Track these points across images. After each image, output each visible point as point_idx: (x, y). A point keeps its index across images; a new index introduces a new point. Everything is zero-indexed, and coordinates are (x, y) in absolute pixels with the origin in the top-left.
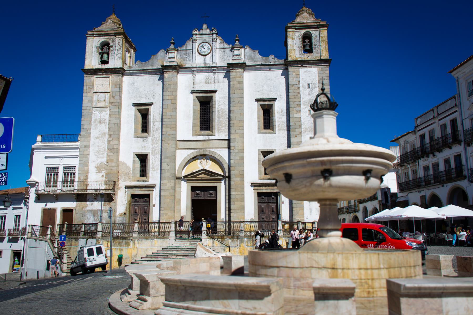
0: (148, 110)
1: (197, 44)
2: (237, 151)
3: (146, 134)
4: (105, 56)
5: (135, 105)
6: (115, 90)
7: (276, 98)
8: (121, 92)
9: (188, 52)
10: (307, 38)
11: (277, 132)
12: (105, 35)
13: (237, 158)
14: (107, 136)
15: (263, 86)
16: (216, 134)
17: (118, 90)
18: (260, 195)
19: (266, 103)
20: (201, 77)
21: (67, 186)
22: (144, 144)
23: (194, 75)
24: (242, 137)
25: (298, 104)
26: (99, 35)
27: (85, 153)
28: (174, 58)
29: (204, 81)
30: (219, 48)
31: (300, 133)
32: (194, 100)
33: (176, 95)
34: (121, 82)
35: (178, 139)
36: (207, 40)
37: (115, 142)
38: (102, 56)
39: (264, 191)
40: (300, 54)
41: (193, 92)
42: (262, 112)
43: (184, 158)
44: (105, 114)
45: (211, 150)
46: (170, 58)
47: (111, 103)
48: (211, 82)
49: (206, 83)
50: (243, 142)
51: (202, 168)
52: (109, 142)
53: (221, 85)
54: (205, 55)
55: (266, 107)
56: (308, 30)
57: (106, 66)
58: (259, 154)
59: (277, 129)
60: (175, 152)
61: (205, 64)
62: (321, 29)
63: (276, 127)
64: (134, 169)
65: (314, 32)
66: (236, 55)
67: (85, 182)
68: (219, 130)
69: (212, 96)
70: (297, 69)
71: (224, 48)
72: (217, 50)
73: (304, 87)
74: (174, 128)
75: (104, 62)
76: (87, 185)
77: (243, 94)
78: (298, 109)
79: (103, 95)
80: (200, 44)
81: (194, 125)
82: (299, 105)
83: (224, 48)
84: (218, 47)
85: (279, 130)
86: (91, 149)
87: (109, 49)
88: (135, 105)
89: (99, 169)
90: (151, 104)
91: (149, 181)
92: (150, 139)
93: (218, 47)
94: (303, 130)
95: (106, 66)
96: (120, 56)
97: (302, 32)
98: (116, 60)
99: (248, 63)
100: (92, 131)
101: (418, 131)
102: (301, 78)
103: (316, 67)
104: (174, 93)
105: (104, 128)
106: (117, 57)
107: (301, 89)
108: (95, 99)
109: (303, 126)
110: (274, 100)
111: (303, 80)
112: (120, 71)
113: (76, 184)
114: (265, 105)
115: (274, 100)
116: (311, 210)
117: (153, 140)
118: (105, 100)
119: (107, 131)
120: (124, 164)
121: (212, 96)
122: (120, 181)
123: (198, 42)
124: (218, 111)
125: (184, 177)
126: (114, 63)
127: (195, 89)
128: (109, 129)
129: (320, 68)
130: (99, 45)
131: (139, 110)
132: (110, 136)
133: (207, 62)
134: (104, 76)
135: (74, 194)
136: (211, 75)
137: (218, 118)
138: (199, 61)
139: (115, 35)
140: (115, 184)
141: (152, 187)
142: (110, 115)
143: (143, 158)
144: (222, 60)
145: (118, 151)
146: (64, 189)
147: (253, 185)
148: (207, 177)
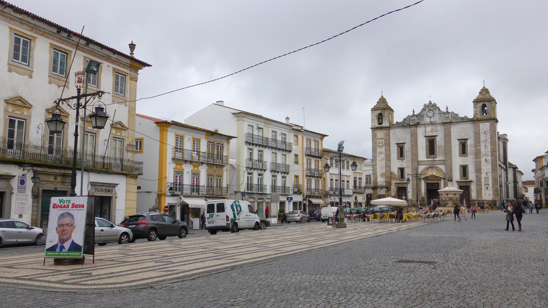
0: (403, 146)
1: (426, 112)
2: (448, 166)
3: (402, 158)
4: (380, 120)
5: (397, 144)
6: (386, 137)
7: (468, 139)
8: (389, 138)
9: (422, 116)
10: (484, 106)
11: (469, 155)
12: (380, 110)
13: (448, 169)
14: (384, 160)
15: (461, 132)
16: (438, 157)
17: (388, 137)
19: (463, 141)
20: (429, 129)
22: (402, 163)
23: (425, 128)
24: (451, 159)
25: (479, 142)
26: (377, 110)
27: (375, 168)
28: (415, 120)
29: (430, 131)
30: (438, 113)
31: (480, 156)
32: (426, 140)
33: (417, 139)
34: (389, 132)
35: (419, 160)
36: (431, 109)
37: (389, 163)
38: (379, 121)
39: (463, 185)
40: (480, 116)
41: (425, 137)
43: (421, 170)
44: (383, 149)
46: (413, 120)
47: (385, 144)
48: (434, 132)
49: (432, 132)
50: (451, 162)
51: (431, 174)
52: (386, 163)
53: (439, 132)
54: (430, 118)
56: (484, 103)
57: (381, 125)
58: (460, 167)
59: (469, 154)
60: (418, 167)
61: (431, 122)
62: (491, 102)
63: (468, 152)
64: (398, 175)
65: (487, 104)
66: (447, 117)
67: (375, 182)
68: (439, 155)
69: (435, 138)
71: (440, 113)
72: (437, 114)
73: (482, 133)
74: (417, 156)
77: (451, 137)
78: (479, 144)
79: (381, 140)
81: (427, 153)
82: (480, 142)
83: (440, 113)
84: (437, 113)
85: (470, 154)
86: (378, 166)
87: (382, 116)
88: (397, 144)
89: (382, 175)
90: (404, 143)
92: (405, 160)
93: (437, 113)
94: (482, 155)
95: (381, 125)
96: (388, 120)
97: (481, 104)
98: (386, 123)
99: (453, 121)
100: (377, 158)
102: (481, 128)
103: (488, 122)
104: (416, 138)
105: (383, 156)
106: (386, 121)
107: (481, 134)
108: (377, 142)
109: (482, 153)
110: (467, 139)
111: (481, 129)
112: (389, 128)
113: (372, 183)
115: (467, 139)
116: (485, 194)
117: (406, 161)
118: (382, 143)
119: (384, 157)
120: (394, 173)
121: (435, 138)
122: (392, 181)
123: (427, 111)
124: (438, 146)
125: (423, 178)
126: (385, 124)
127: (426, 135)
128: (385, 157)
130: (377, 114)
131: (399, 146)
132: (386, 160)
133: (432, 121)
136: (434, 127)
137: (438, 149)
138: (428, 120)
139: (385, 109)
140: (390, 183)
142: (385, 150)
143: (402, 170)
144: (439, 119)
145: (390, 167)
147: (457, 182)
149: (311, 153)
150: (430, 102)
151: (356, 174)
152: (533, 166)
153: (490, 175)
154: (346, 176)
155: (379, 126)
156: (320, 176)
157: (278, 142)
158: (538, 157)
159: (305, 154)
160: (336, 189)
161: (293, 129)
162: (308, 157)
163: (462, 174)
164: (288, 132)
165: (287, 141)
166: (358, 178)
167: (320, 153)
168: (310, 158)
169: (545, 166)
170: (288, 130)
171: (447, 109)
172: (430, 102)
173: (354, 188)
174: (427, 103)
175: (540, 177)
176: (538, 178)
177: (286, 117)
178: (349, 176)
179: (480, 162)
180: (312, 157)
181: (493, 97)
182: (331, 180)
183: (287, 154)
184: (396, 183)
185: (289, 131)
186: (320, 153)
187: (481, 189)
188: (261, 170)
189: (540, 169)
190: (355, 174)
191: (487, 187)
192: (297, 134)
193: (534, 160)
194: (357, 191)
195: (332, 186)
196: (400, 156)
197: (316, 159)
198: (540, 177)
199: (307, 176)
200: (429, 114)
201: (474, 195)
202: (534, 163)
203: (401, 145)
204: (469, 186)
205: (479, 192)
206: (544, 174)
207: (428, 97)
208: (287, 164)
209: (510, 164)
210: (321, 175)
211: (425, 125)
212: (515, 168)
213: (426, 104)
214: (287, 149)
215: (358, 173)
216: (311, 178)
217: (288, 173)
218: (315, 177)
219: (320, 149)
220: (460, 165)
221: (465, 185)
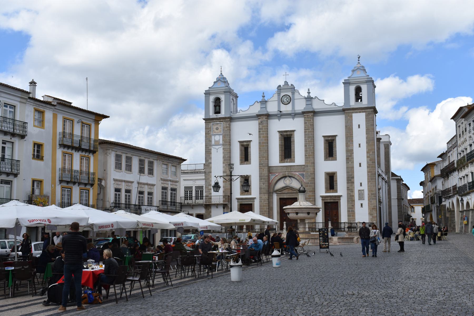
0: (248, 145)
4: (217, 107)
10: (358, 90)
18: (325, 202)
19: (330, 139)
21: (198, 199)
39: (329, 201)
42: (328, 145)
44: (221, 150)
45: (292, 173)
55: (330, 141)
57: (219, 116)
70: (351, 114)
75: (217, 111)
76: (211, 198)
80: (283, 96)
81: (281, 155)
91: (251, 194)
95: (219, 116)
101: (448, 153)
113: (204, 197)
114: (329, 140)
129: (367, 113)
134: (218, 123)
135: (204, 204)
141: (254, 199)
146: (197, 201)
147: (322, 197)
148: (290, 191)
149: (72, 142)
150: (286, 83)
151: (167, 182)
152: (422, 177)
153: (365, 187)
154: (147, 184)
155: (215, 116)
156: (91, 182)
157: (18, 123)
158: (427, 165)
159: (60, 145)
160: (125, 204)
161: (30, 98)
162: (66, 150)
163: (329, 185)
164: (20, 102)
165: (18, 118)
166: (169, 188)
167: (92, 146)
168: (70, 151)
169: (438, 176)
170: (19, 99)
171: (309, 93)
172: (286, 83)
173: (162, 204)
174: (282, 84)
175: (430, 192)
176: (428, 193)
177: (31, 81)
178: (153, 185)
179: (353, 167)
180: (73, 152)
181: (370, 77)
182: (118, 190)
183: (16, 140)
184: (238, 199)
185: (24, 101)
186: (92, 146)
187: (353, 206)
188: (8, 174)
189: (431, 181)
190: (164, 182)
191: (362, 205)
192: (42, 109)
193: (422, 170)
194: (167, 209)
195: (119, 201)
196: (244, 159)
197: (84, 154)
198: (430, 192)
199: (61, 181)
200: (285, 101)
201: (344, 218)
202: (423, 173)
203: (245, 144)
204: (337, 202)
205: (351, 212)
206: (436, 187)
207: (284, 75)
208: (16, 158)
209: (393, 175)
210: (94, 180)
211: (280, 115)
212: (399, 180)
213: (280, 86)
214: (17, 132)
215: (170, 181)
216: (70, 185)
217: (16, 175)
218: (80, 184)
219: (93, 137)
220: (325, 172)
221: (332, 201)
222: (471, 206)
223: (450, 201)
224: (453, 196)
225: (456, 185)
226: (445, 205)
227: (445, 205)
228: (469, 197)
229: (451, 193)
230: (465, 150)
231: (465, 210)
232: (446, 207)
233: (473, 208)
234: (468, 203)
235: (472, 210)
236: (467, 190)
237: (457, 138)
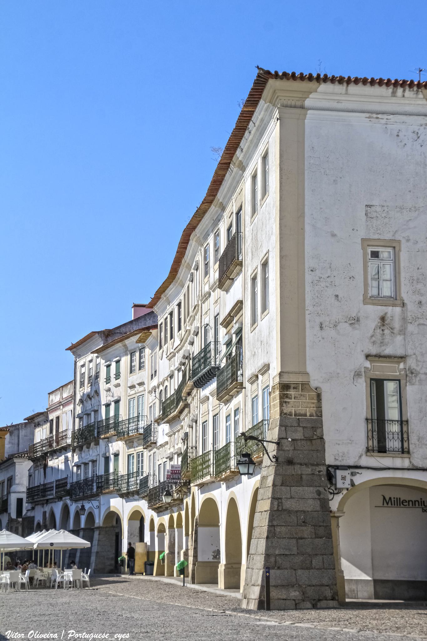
222: (97, 521)
223: (47, 509)
224: (53, 501)
225: (66, 478)
226: (34, 517)
227: (34, 517)
228: (95, 503)
229: (52, 494)
230: (93, 413)
231: (82, 529)
232: (33, 521)
233: (101, 525)
234: (91, 517)
235: (99, 528)
236: (92, 489)
237: (75, 388)
